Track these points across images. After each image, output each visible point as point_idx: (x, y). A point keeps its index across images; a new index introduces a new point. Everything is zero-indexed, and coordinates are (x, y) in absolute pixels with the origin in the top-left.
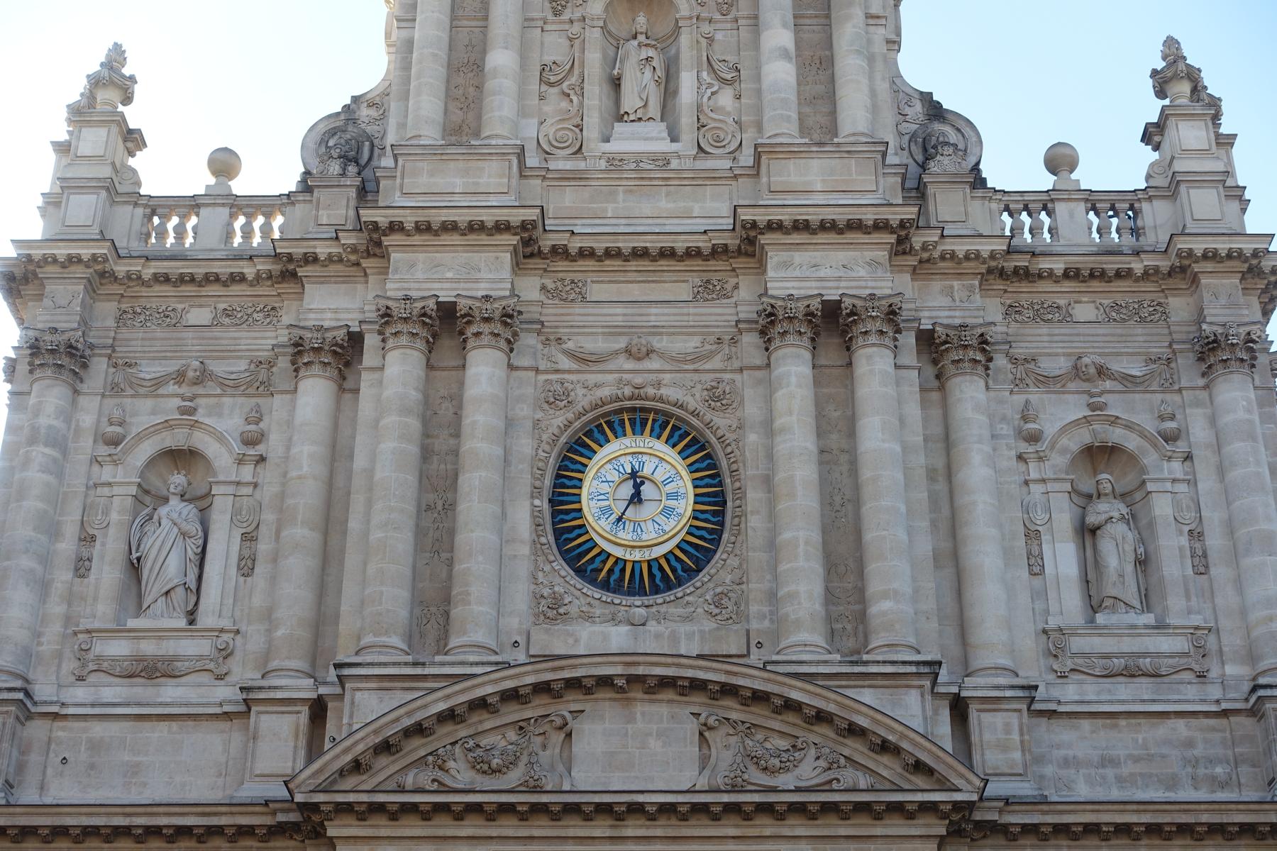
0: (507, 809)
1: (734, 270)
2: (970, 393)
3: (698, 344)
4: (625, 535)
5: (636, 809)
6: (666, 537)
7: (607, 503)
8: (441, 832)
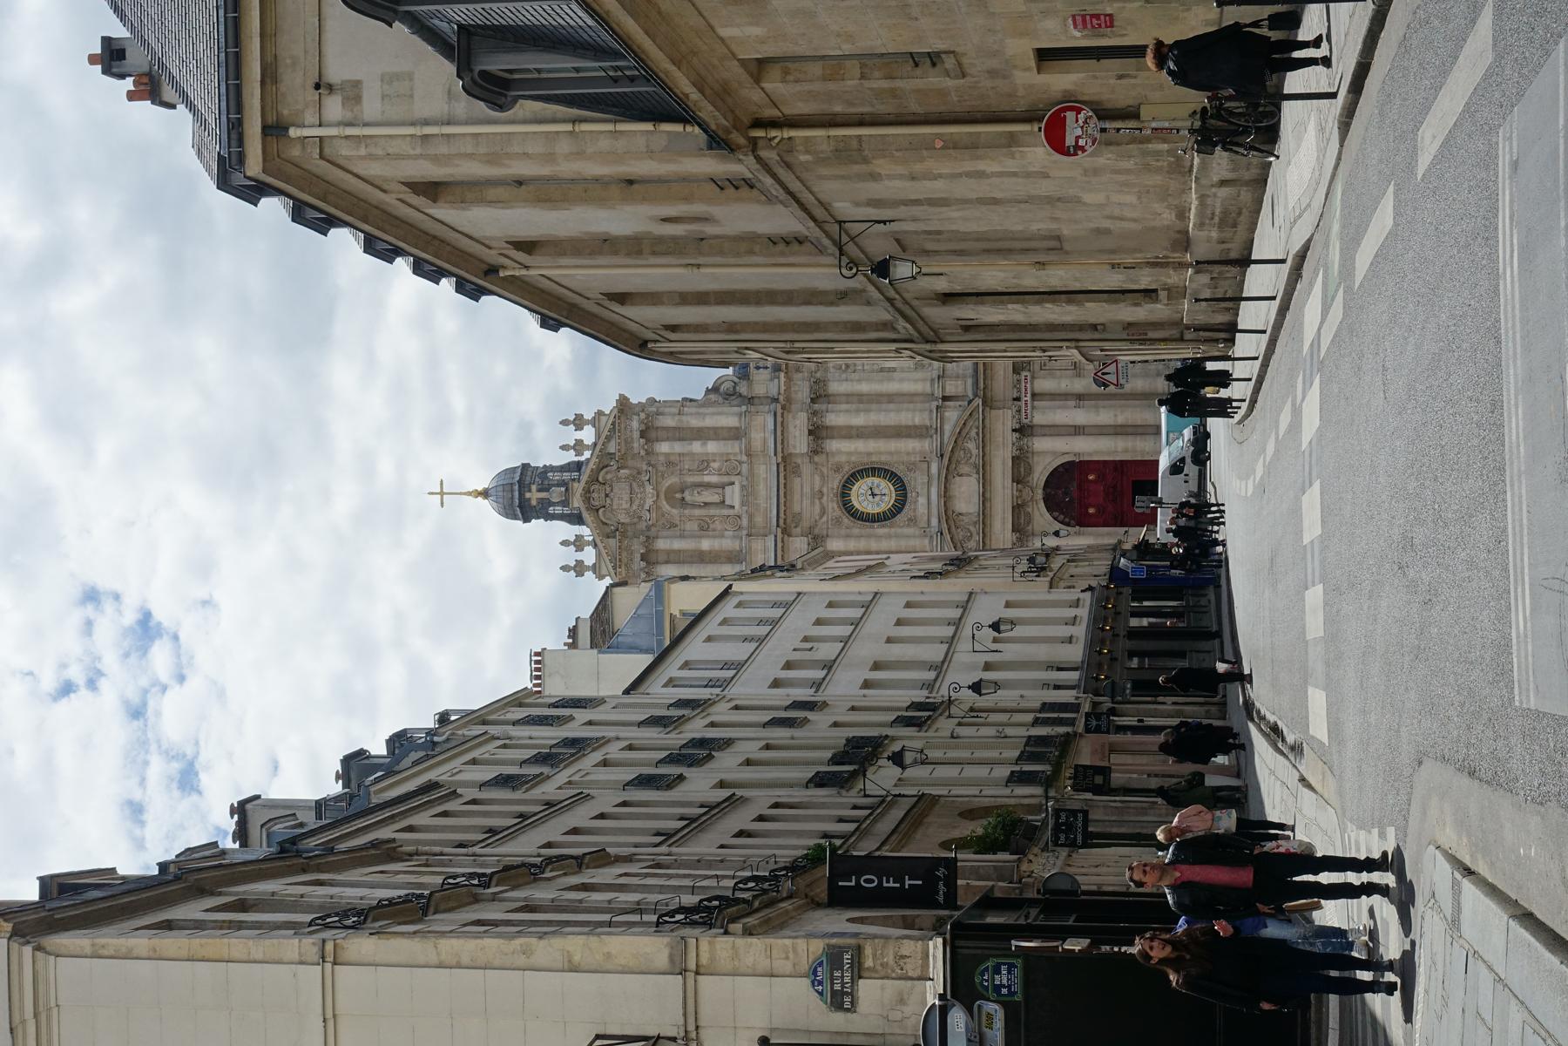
2: (835, 387)
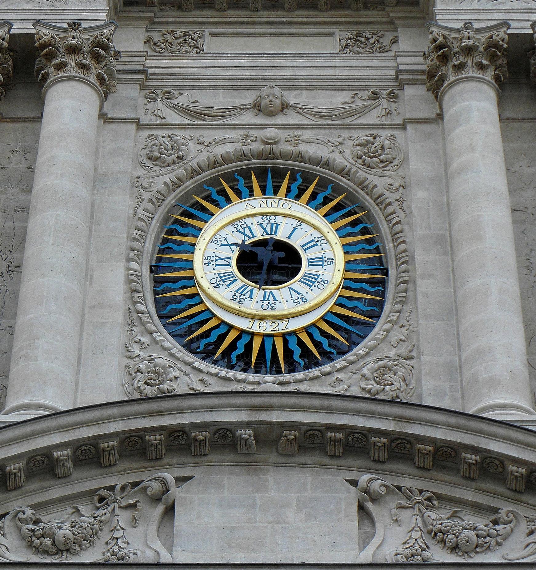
1: (391, 22)
3: (348, 100)
4: (252, 306)
6: (307, 306)
7: (227, 269)
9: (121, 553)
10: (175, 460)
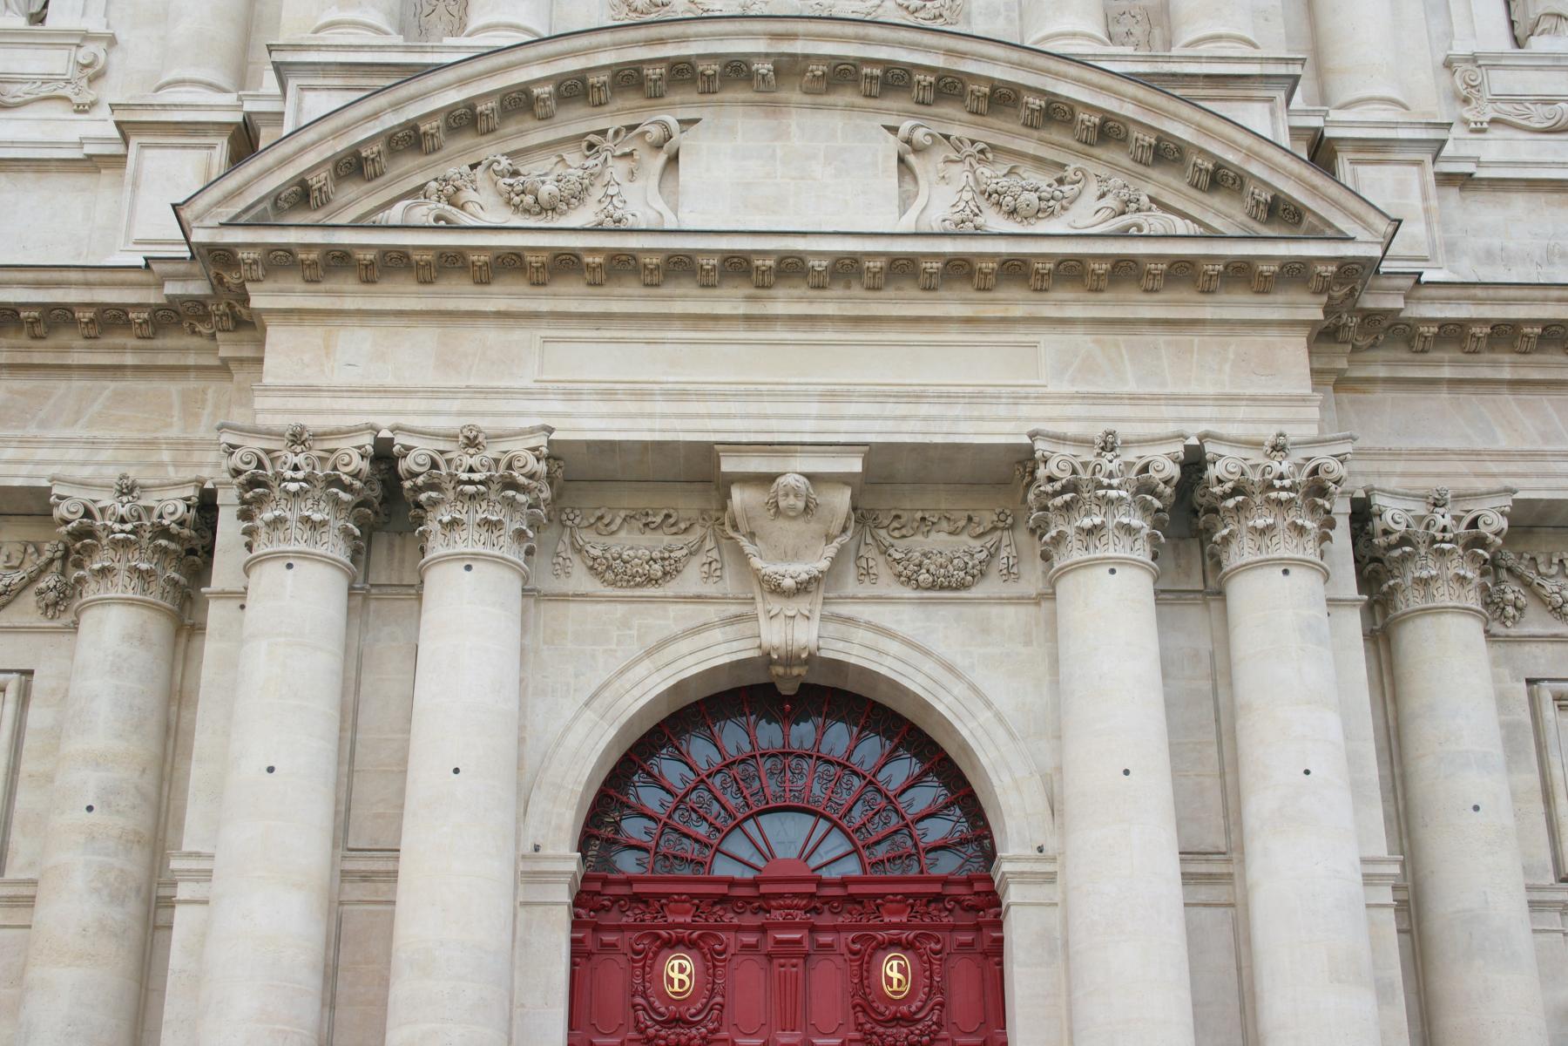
0: (565, 265)
5: (791, 268)
8: (450, 304)
9: (617, 215)
10: (677, 98)
